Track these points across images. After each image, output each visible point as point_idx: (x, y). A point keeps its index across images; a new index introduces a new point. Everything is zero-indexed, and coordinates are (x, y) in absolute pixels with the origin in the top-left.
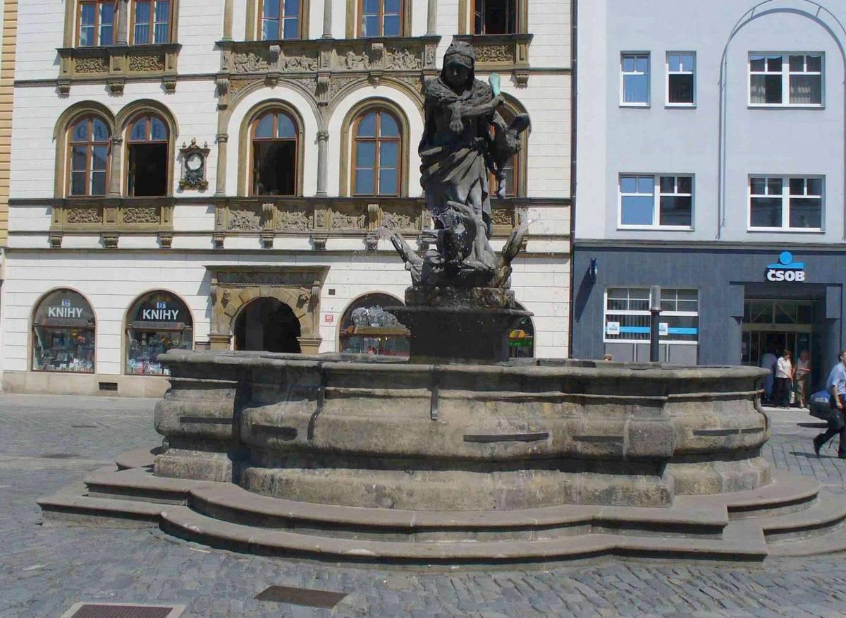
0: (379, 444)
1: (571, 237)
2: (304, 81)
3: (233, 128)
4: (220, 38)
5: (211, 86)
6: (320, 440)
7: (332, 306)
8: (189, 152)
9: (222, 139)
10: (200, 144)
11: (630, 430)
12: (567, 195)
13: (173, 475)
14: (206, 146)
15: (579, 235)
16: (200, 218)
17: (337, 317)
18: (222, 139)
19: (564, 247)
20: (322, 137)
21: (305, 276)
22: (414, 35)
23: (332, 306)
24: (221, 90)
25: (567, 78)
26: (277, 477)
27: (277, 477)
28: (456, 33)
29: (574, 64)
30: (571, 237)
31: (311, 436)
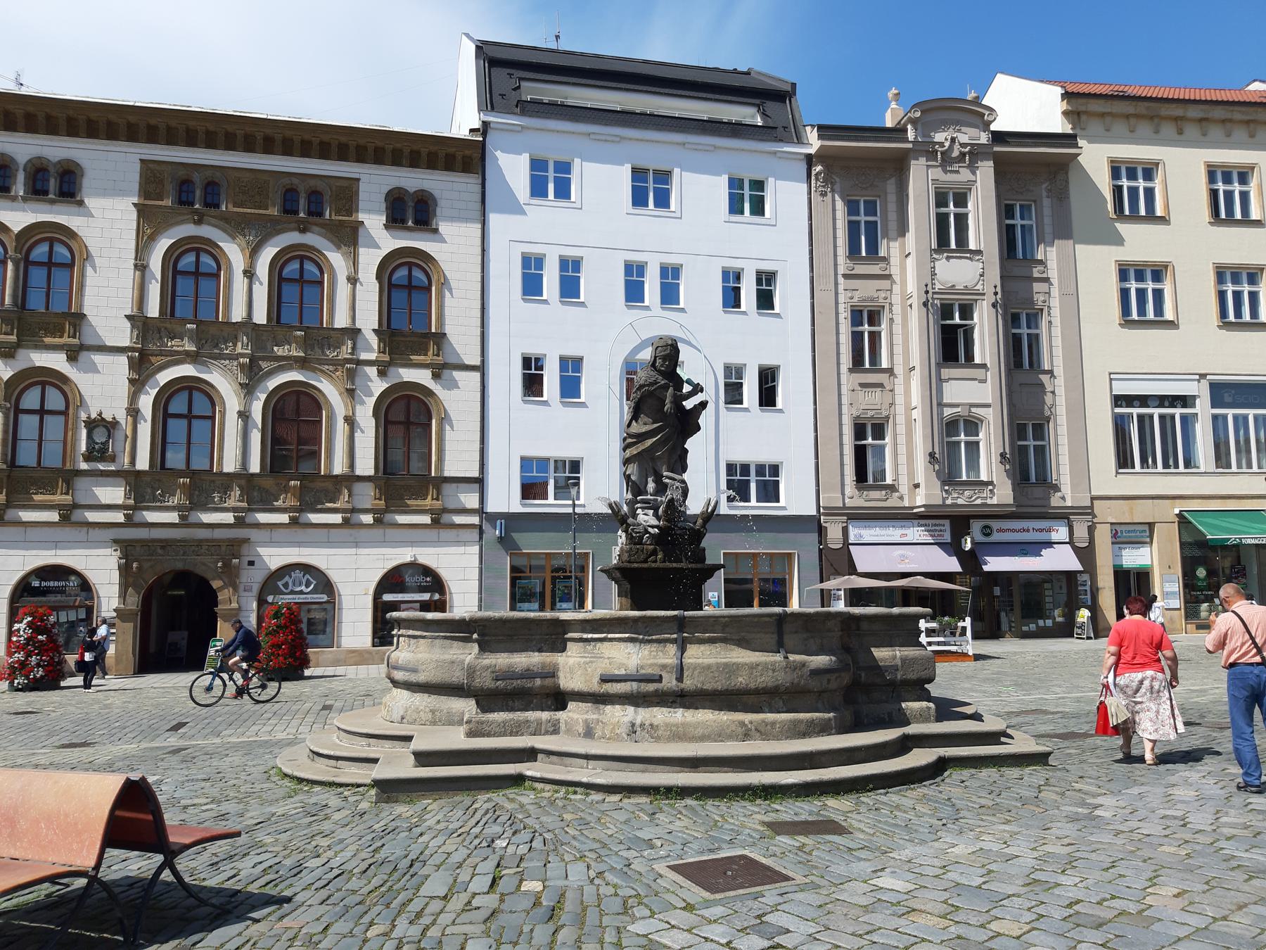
0: (744, 682)
1: (481, 511)
2: (223, 361)
3: (146, 403)
4: (128, 312)
5: (123, 361)
6: (689, 683)
7: (253, 578)
8: (92, 425)
9: (134, 412)
10: (108, 416)
11: (901, 659)
12: (476, 474)
13: (489, 735)
14: (114, 418)
15: (491, 508)
16: (114, 494)
17: (256, 588)
18: (134, 412)
19: (475, 520)
20: (244, 415)
21: (223, 548)
22: (336, 326)
23: (253, 578)
24: (133, 365)
25: (477, 375)
26: (638, 722)
27: (638, 722)
28: (377, 328)
29: (483, 362)
30: (481, 511)
31: (680, 679)
